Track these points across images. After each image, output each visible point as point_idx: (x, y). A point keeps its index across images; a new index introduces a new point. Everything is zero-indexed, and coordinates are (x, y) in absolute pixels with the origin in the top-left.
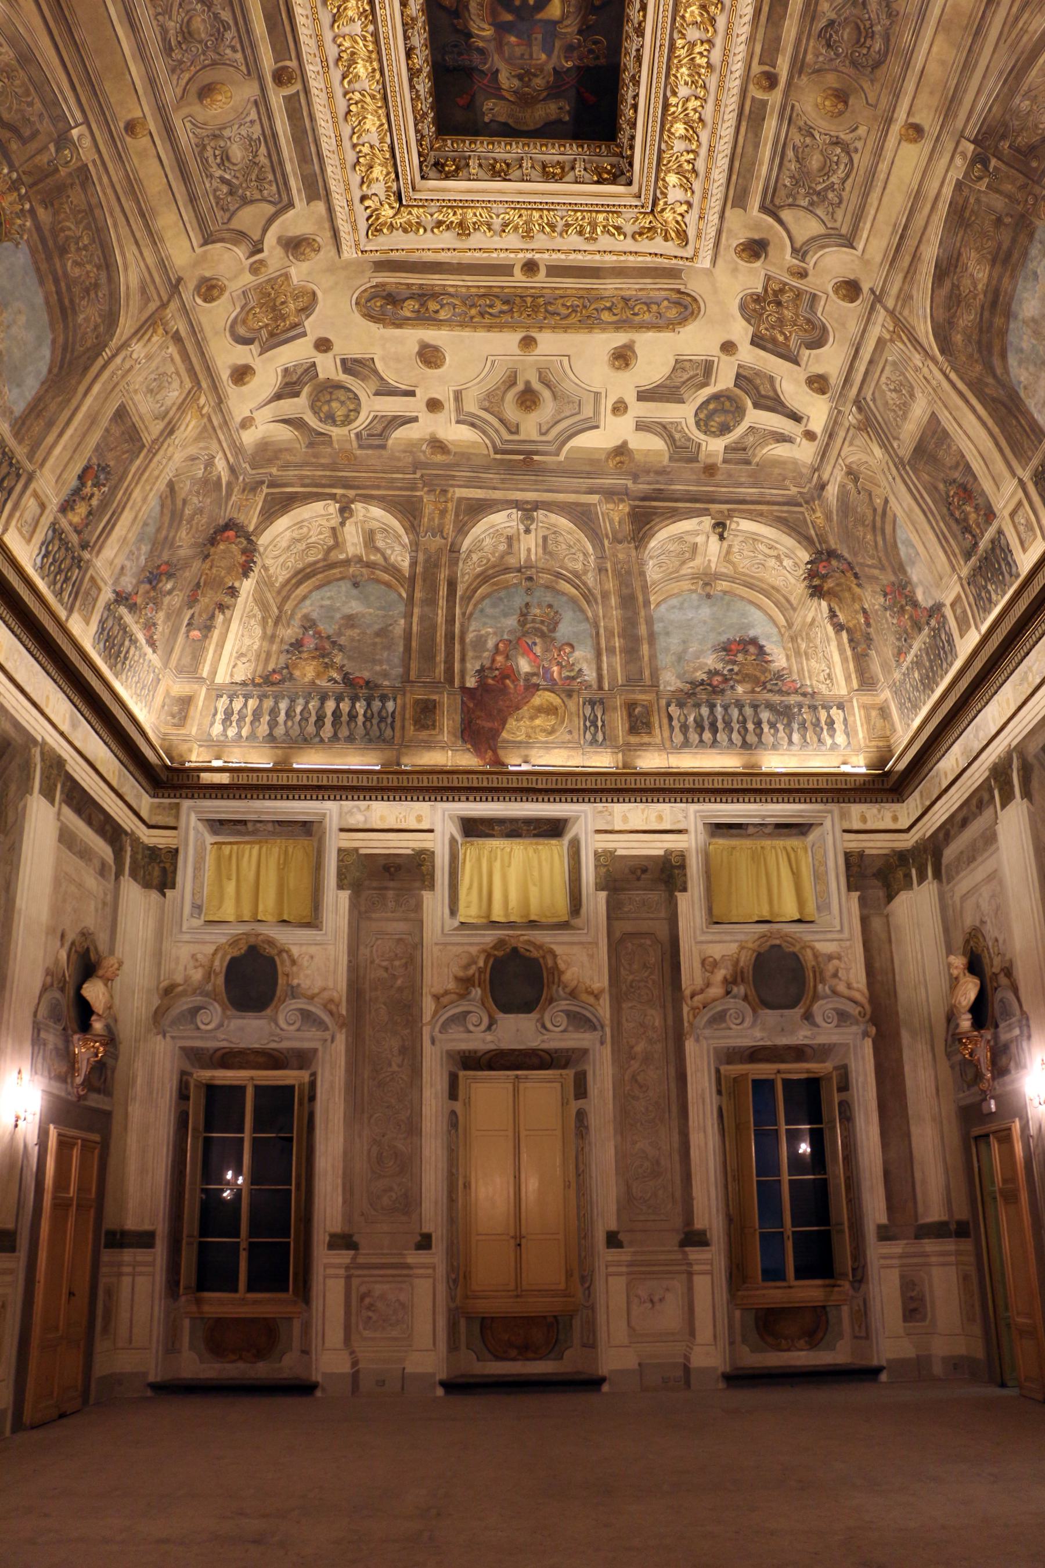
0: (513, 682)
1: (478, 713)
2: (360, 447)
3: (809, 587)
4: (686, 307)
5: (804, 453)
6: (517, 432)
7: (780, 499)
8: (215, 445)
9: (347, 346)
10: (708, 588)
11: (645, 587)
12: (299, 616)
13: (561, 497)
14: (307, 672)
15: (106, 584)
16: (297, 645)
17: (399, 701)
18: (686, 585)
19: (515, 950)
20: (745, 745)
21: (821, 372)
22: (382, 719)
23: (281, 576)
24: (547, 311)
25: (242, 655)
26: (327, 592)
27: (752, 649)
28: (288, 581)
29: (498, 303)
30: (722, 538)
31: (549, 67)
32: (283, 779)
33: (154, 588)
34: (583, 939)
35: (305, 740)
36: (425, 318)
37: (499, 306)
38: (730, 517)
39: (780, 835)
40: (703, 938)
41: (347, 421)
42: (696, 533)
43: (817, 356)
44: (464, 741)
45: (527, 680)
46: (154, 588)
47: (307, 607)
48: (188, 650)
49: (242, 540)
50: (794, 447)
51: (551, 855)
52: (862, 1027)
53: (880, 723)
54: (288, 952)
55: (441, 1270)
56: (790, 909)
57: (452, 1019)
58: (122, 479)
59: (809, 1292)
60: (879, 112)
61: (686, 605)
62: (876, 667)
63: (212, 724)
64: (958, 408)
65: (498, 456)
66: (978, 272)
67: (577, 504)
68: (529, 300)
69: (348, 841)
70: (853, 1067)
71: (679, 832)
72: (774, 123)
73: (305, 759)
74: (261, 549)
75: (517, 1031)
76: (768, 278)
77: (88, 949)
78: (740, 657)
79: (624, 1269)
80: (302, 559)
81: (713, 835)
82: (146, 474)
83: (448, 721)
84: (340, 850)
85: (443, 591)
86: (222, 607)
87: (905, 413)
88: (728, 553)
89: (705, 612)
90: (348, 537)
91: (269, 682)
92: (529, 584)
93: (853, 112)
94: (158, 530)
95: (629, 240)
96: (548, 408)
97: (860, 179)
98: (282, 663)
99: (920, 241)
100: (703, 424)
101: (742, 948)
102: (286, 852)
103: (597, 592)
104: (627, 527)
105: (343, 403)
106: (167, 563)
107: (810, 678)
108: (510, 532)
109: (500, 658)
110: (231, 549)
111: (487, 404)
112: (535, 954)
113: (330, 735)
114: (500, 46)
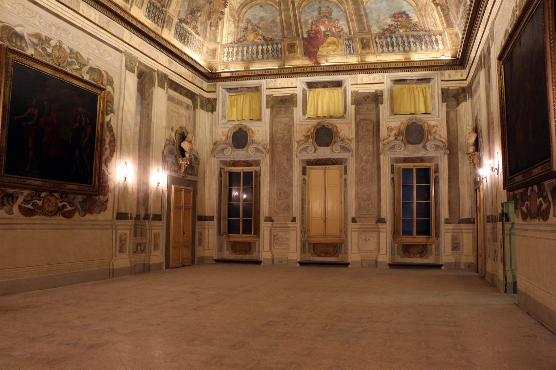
12: (245, 19)
14: (251, 37)
16: (246, 29)
19: (324, 126)
20: (405, 51)
22: (277, 51)
23: (237, 6)
26: (253, 10)
28: (239, 7)
32: (247, 74)
33: (193, 16)
34: (346, 121)
39: (419, 83)
40: (388, 120)
45: (324, 33)
46: (193, 16)
47: (247, 16)
48: (212, 34)
51: (337, 93)
52: (444, 151)
54: (251, 129)
55: (299, 228)
56: (423, 110)
57: (303, 149)
59: (421, 239)
62: (452, 19)
63: (224, 57)
69: (269, 92)
70: (440, 165)
71: (381, 83)
73: (254, 66)
75: (324, 153)
77: (183, 132)
78: (400, 19)
79: (357, 230)
81: (395, 84)
83: (299, 49)
84: (267, 95)
85: (291, 5)
86: (220, 19)
91: (239, 42)
101: (402, 123)
102: (252, 97)
106: (196, 7)
109: (314, 27)
112: (330, 127)
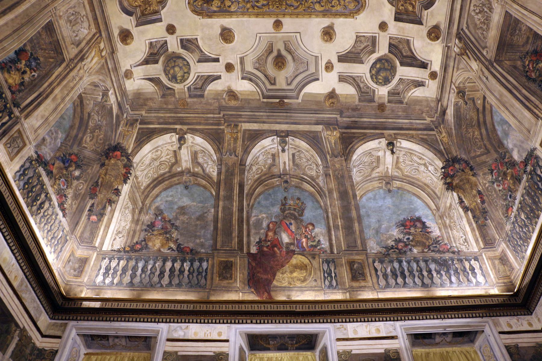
0: (279, 249)
1: (258, 269)
2: (190, 96)
3: (445, 183)
6: (274, 84)
7: (421, 126)
8: (109, 82)
9: (183, 32)
10: (389, 186)
11: (352, 186)
12: (154, 207)
13: (301, 127)
14: (156, 243)
15: (30, 143)
16: (151, 226)
17: (210, 262)
18: (376, 184)
20: (424, 285)
21: (434, 24)
22: (199, 273)
23: (145, 182)
24: (286, 4)
25: (120, 232)
26: (170, 192)
27: (419, 225)
28: (149, 185)
30: (393, 153)
33: (66, 168)
35: (152, 286)
38: (396, 139)
41: (184, 79)
42: (378, 149)
43: (432, 12)
44: (250, 287)
45: (287, 248)
46: (66, 168)
47: (158, 202)
48: (88, 228)
49: (124, 158)
50: (426, 87)
53: (501, 268)
58: (48, 75)
61: (377, 197)
62: (493, 231)
63: (97, 276)
65: (265, 100)
67: (311, 132)
71: (392, 338)
74: (135, 165)
78: (412, 230)
80: (157, 172)
82: (65, 83)
83: (240, 275)
84: (165, 353)
86: (110, 202)
87: (488, 26)
88: (397, 162)
89: (389, 201)
90: (183, 156)
91: (134, 250)
92: (286, 185)
94: (72, 127)
96: (290, 68)
98: (142, 238)
100: (374, 77)
103: (325, 190)
104: (340, 147)
105: (181, 68)
106: (76, 155)
107: (455, 242)
108: (274, 151)
109: (270, 234)
110: (116, 163)
113: (167, 282)
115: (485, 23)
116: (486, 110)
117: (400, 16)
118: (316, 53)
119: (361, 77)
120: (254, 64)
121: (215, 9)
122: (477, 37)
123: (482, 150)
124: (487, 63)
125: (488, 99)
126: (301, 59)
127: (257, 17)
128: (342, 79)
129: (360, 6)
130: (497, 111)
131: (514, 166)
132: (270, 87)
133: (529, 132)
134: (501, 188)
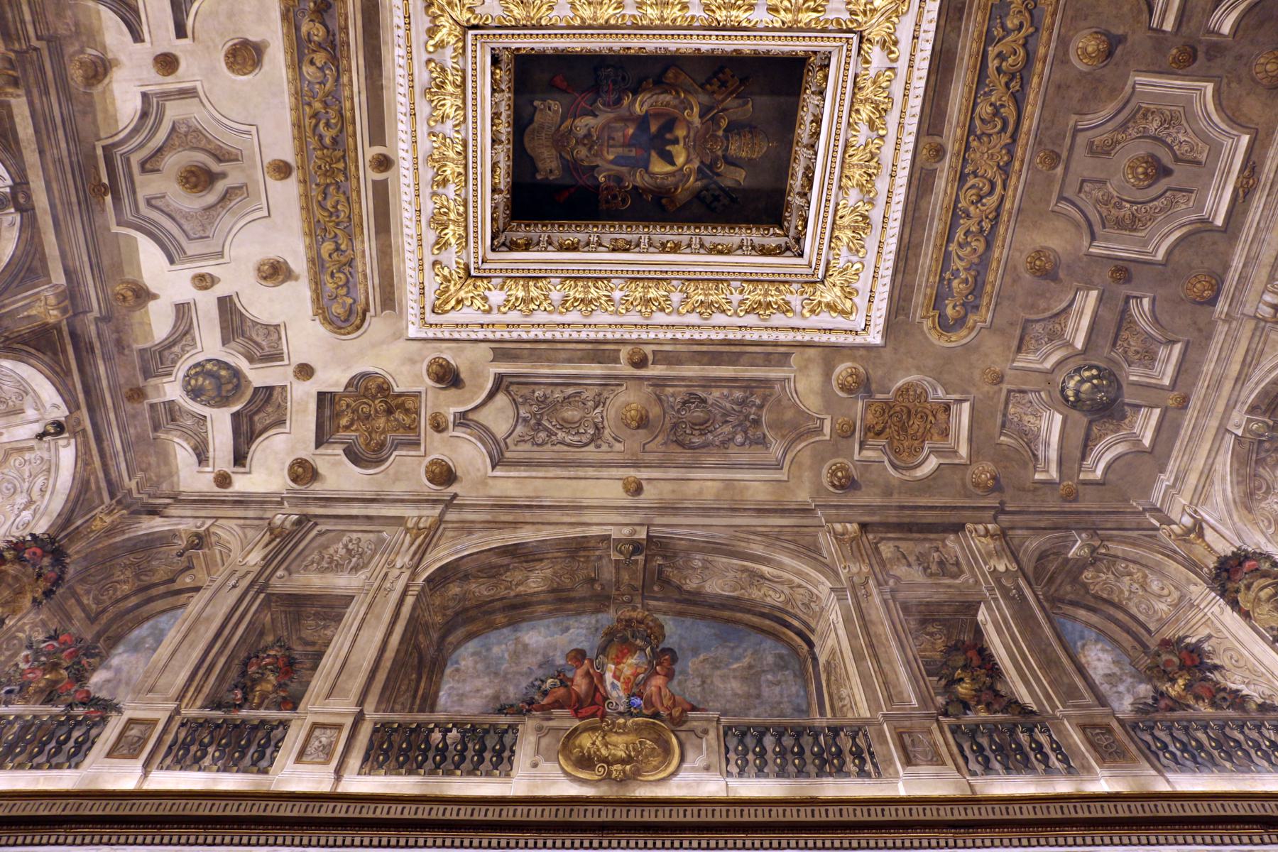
4: (346, 320)
5: (192, 477)
21: (320, 471)
24: (328, 185)
29: (333, 132)
31: (600, 162)
36: (299, 50)
37: (328, 136)
50: (196, 467)
60: (640, 456)
64: (379, 618)
65: (100, 152)
66: (535, 581)
67: (43, 260)
68: (341, 165)
72: (599, 372)
76: (417, 395)
93: (633, 435)
95: (432, 258)
97: (570, 456)
99: (533, 523)
104: (24, 328)
111: (183, 129)
114: (625, 120)
115: (330, 563)
116: (176, 598)
117: (327, 403)
118: (231, 252)
119: (194, 345)
120: (186, 122)
121: (304, 29)
122: (306, 552)
123: (94, 606)
124: (262, 580)
125: (197, 596)
126: (211, 223)
127: (294, 125)
128: (182, 310)
129: (340, 323)
130: (177, 619)
131: (78, 680)
132: (135, 160)
133: (150, 691)
134: (23, 666)
